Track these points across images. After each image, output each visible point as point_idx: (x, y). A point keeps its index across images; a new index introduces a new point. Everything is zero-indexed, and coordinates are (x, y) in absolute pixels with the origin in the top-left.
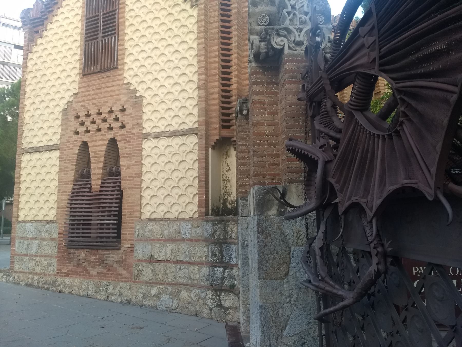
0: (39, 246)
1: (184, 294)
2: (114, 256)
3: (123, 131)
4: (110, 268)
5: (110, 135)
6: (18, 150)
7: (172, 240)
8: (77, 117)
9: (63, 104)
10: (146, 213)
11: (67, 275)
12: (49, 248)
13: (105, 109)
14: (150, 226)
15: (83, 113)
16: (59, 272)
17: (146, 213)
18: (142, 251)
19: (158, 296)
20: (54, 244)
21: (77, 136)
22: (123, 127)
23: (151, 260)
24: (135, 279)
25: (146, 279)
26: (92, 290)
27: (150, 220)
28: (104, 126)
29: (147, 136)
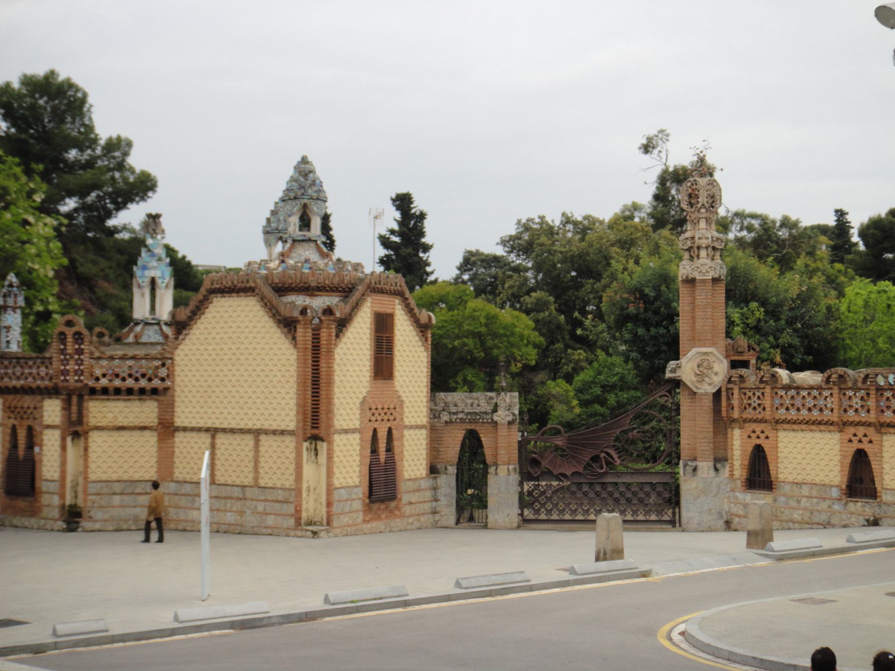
0: (351, 505)
1: (422, 519)
2: (393, 504)
3: (395, 423)
4: (392, 512)
5: (389, 425)
6: (332, 430)
7: (418, 490)
8: (370, 409)
9: (361, 397)
10: (406, 475)
11: (368, 522)
12: (358, 505)
13: (386, 406)
14: (409, 483)
15: (374, 407)
16: (364, 521)
17: (406, 476)
18: (405, 498)
19: (412, 523)
20: (360, 502)
21: (370, 424)
22: (395, 420)
23: (410, 503)
24: (403, 516)
25: (407, 514)
26: (382, 527)
27: (409, 480)
28: (386, 418)
29: (406, 427)
